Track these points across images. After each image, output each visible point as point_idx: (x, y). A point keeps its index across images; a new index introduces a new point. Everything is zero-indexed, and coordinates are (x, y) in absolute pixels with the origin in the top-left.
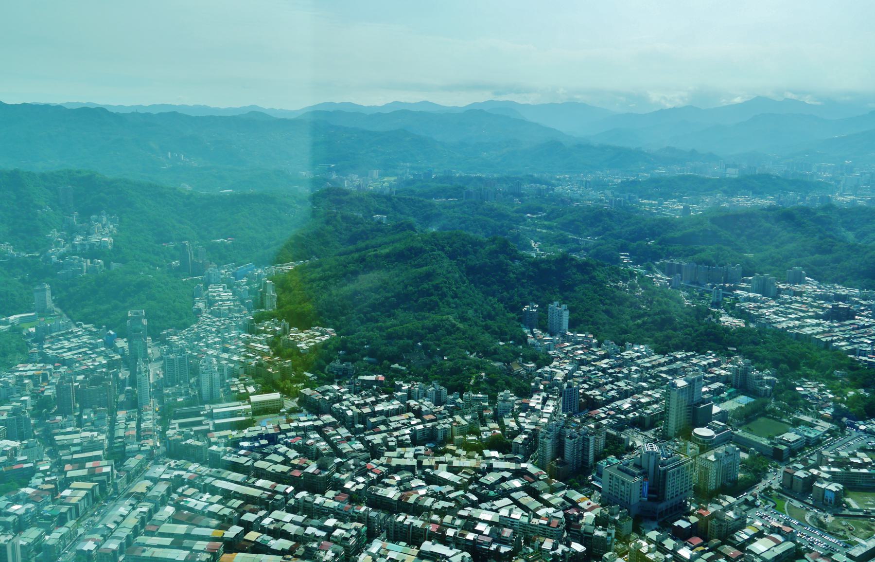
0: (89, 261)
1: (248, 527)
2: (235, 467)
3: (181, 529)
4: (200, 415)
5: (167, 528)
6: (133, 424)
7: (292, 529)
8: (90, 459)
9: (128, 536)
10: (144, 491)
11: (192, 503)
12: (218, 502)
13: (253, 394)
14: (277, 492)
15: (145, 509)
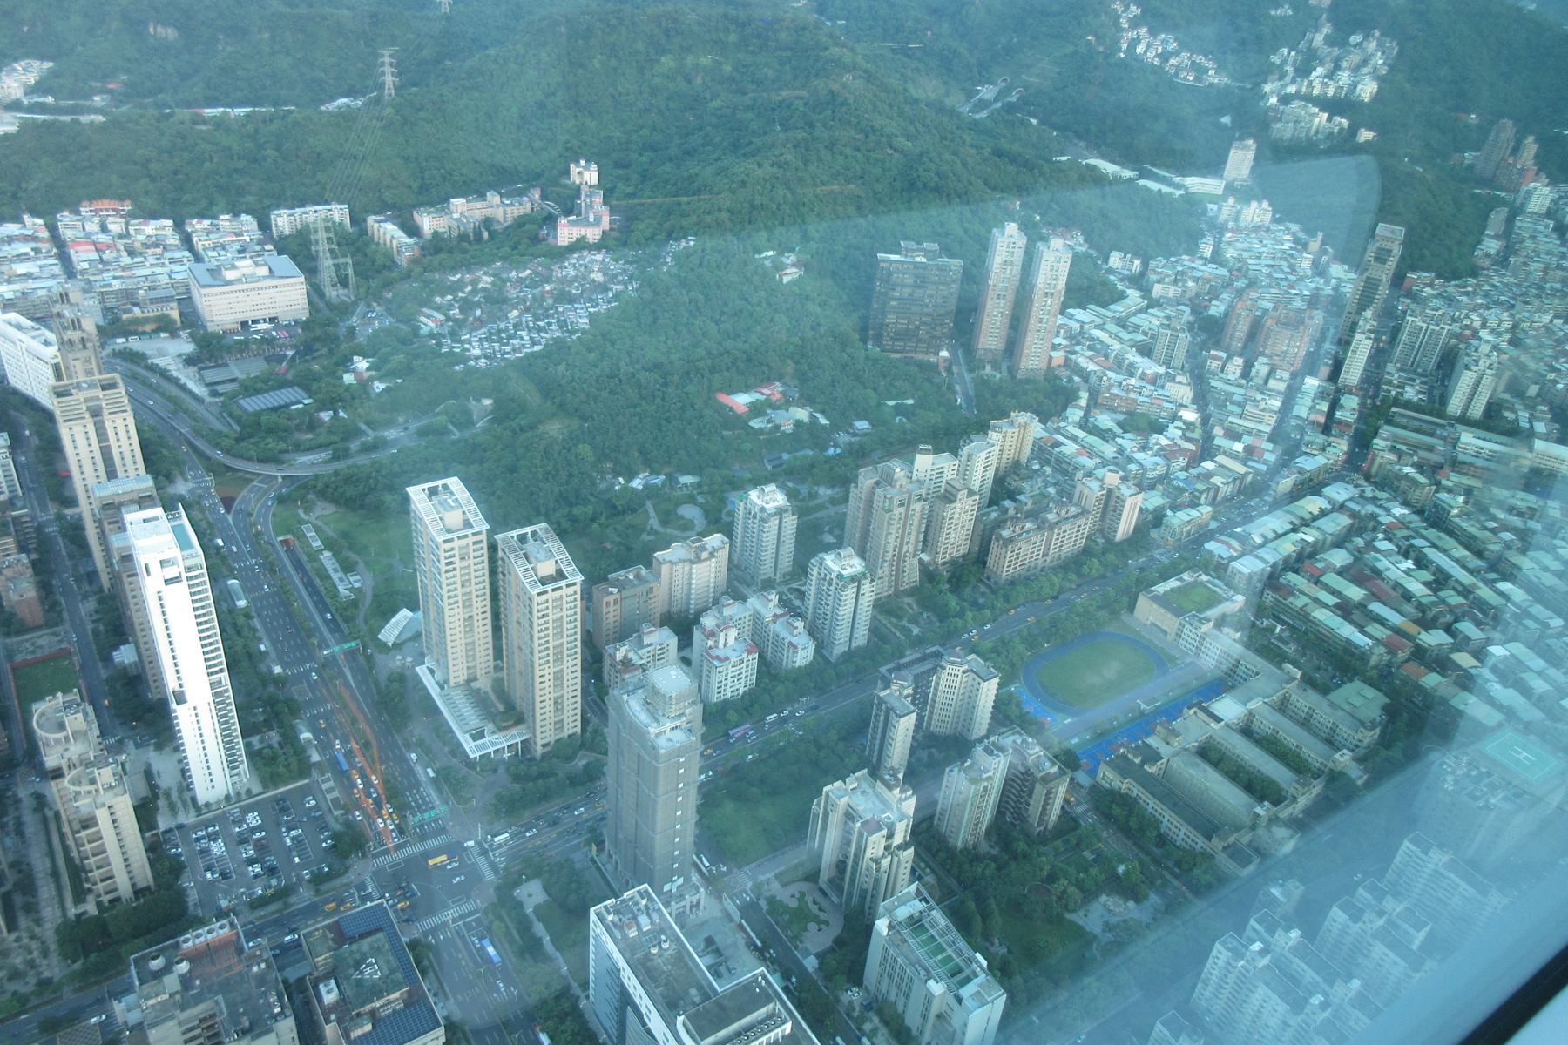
0: (1326, 115)
1: (1461, 643)
2: (1468, 542)
3: (1355, 593)
4: (1432, 435)
5: (1331, 579)
6: (1325, 407)
7: (1539, 686)
8: (1249, 432)
9: (1274, 566)
10: (1316, 512)
11: (1383, 564)
12: (1424, 583)
13: (1546, 437)
14: (1530, 616)
15: (1310, 539)
